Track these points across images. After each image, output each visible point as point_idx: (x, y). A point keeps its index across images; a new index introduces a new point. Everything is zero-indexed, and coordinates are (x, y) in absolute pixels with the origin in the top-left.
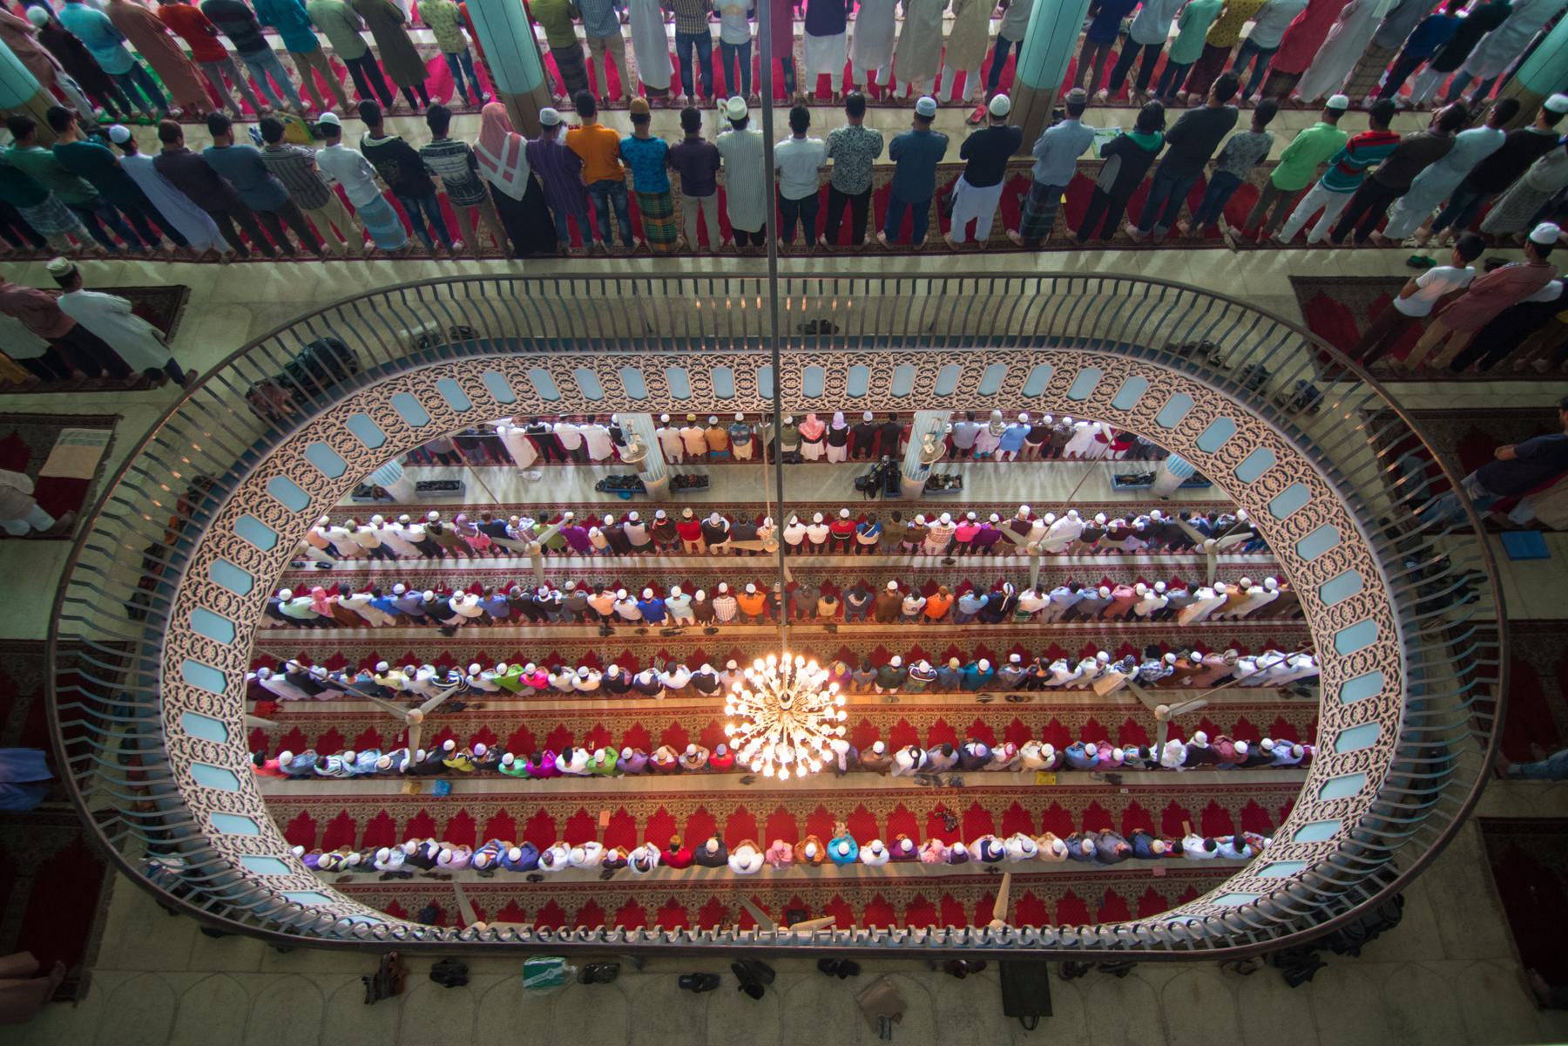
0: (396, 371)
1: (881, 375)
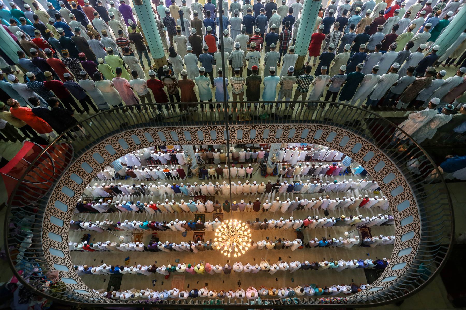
1: (259, 132)
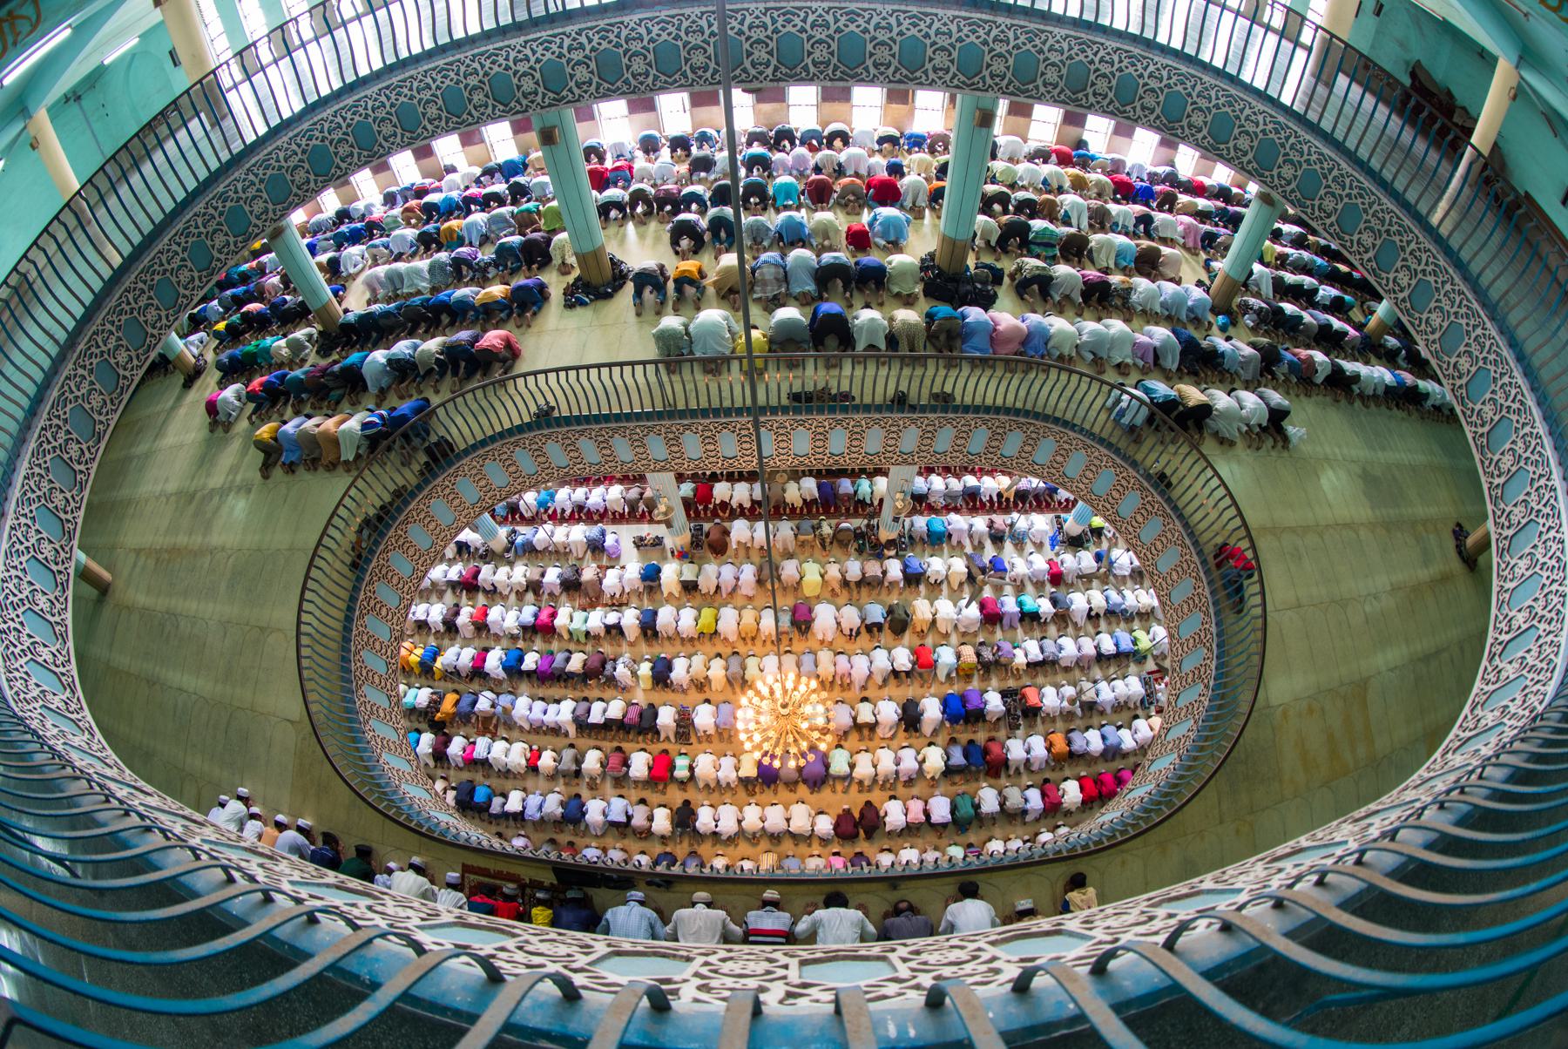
1: (856, 436)
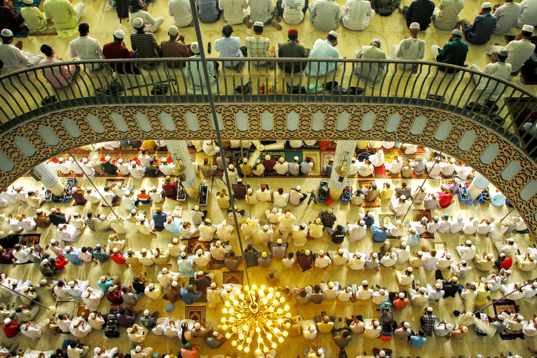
0: (41, 114)
1: (305, 119)
